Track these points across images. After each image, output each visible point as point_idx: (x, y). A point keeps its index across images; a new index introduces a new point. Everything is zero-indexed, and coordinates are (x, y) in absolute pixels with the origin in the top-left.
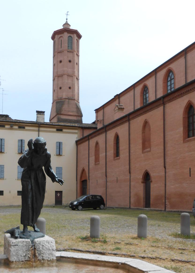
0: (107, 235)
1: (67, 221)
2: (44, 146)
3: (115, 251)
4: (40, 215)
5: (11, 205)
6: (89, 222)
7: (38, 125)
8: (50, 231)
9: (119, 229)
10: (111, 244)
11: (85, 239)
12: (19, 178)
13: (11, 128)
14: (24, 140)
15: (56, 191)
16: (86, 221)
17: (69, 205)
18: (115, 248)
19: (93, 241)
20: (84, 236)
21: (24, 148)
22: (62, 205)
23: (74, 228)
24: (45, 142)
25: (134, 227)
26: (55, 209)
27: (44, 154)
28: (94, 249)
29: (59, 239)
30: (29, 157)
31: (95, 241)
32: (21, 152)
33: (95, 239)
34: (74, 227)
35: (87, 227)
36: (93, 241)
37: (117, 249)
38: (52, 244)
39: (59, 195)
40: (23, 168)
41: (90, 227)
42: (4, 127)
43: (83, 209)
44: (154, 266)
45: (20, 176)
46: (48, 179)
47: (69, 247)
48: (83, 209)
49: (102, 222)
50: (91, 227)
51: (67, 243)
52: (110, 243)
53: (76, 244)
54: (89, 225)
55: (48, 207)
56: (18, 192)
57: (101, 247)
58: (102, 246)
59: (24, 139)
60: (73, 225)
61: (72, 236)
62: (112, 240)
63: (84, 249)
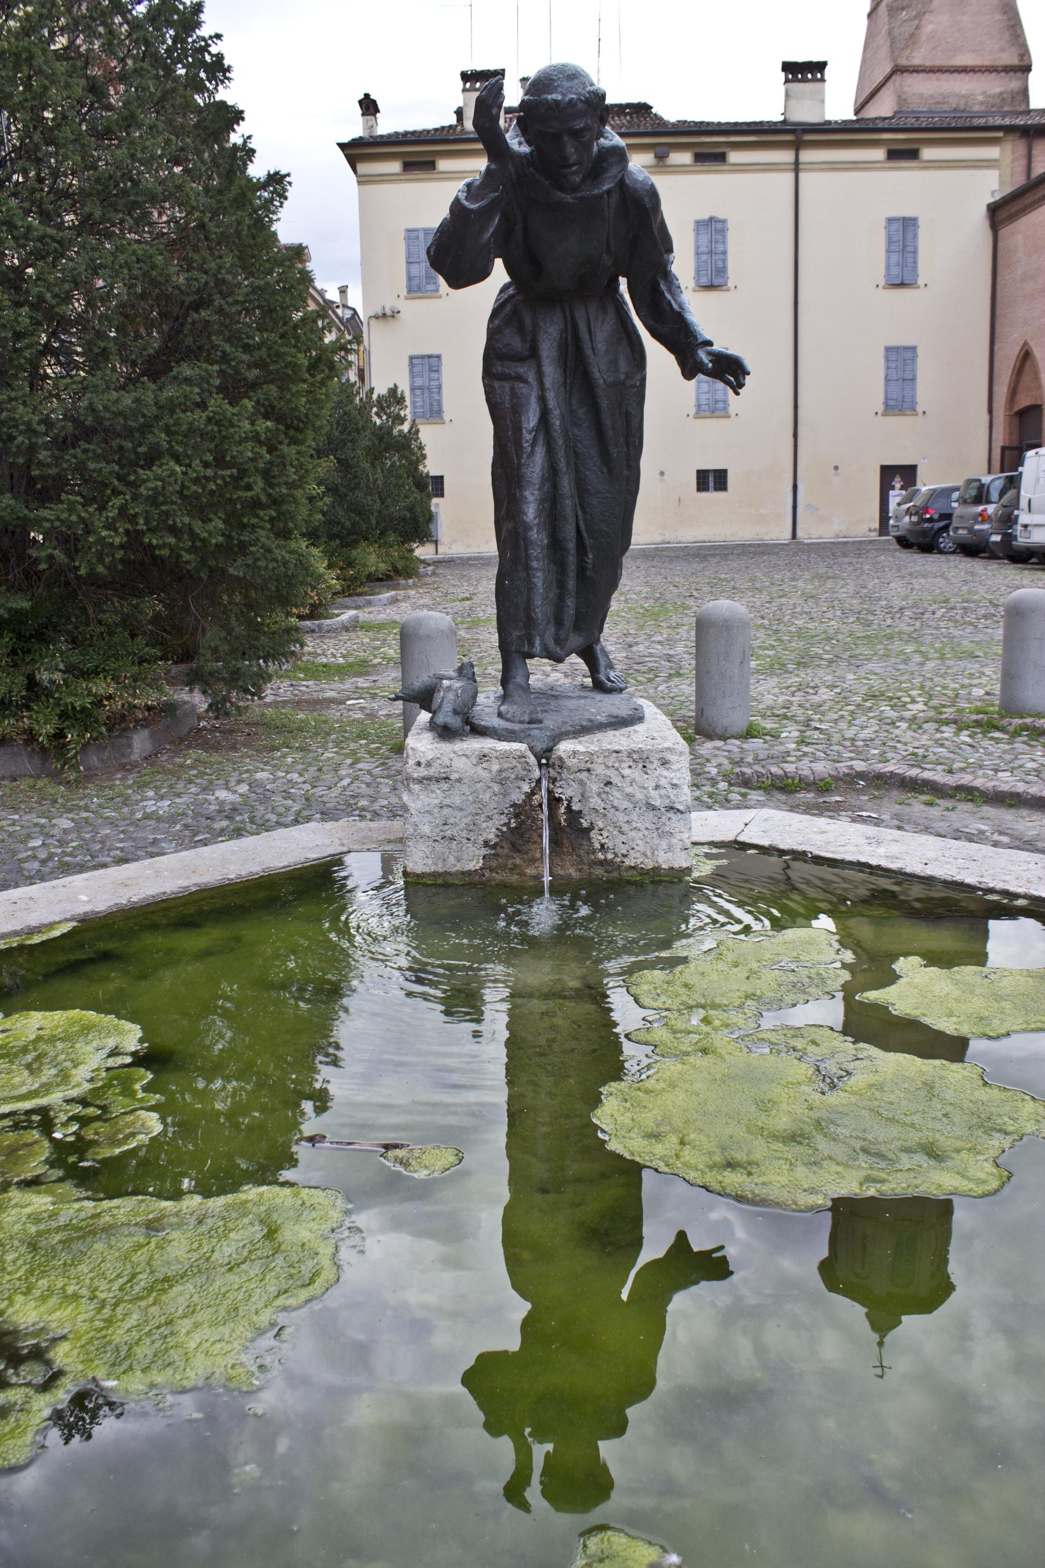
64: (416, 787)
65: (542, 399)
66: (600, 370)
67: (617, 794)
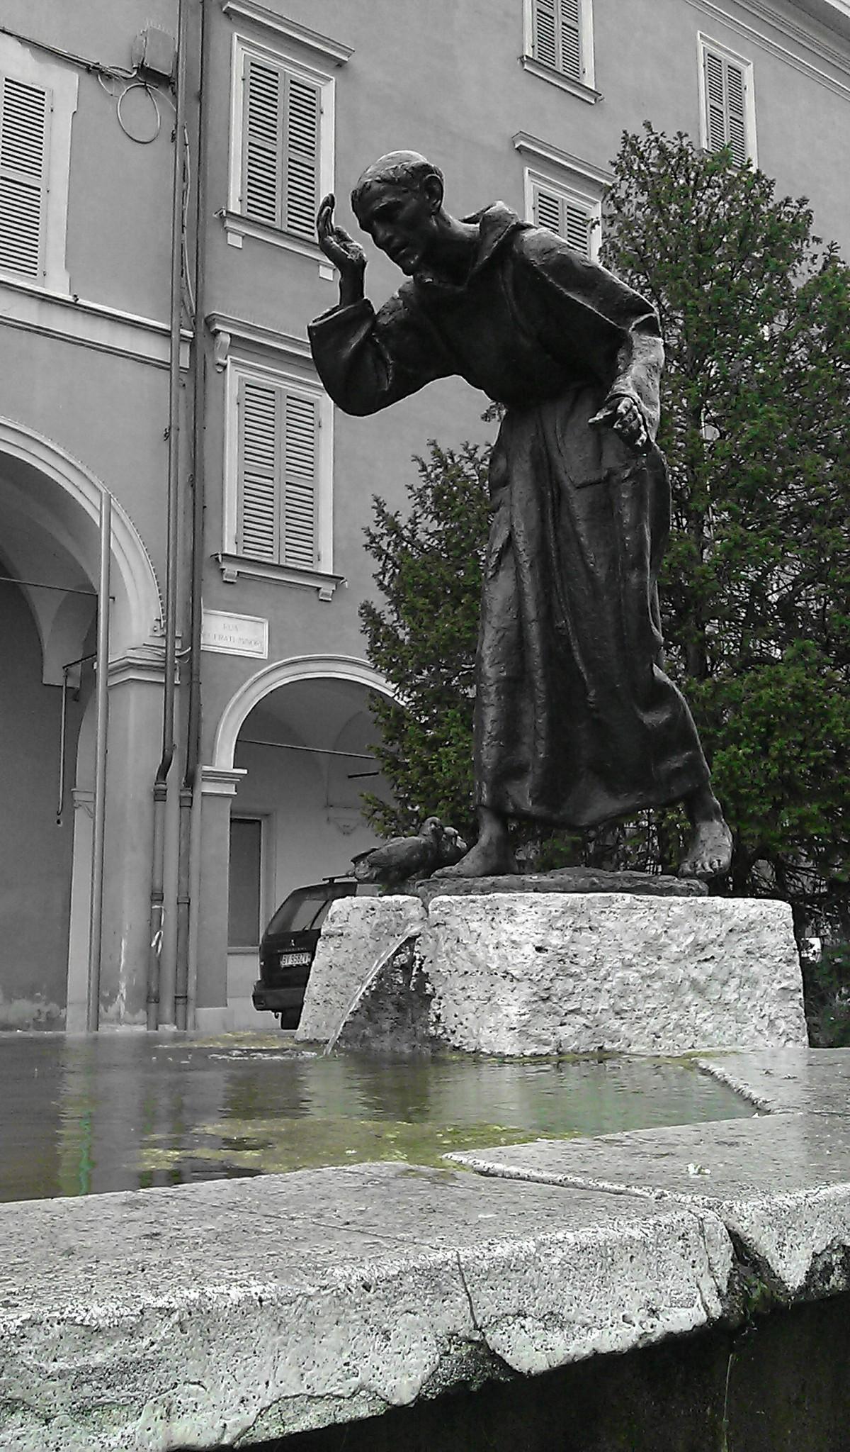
67: (462, 953)
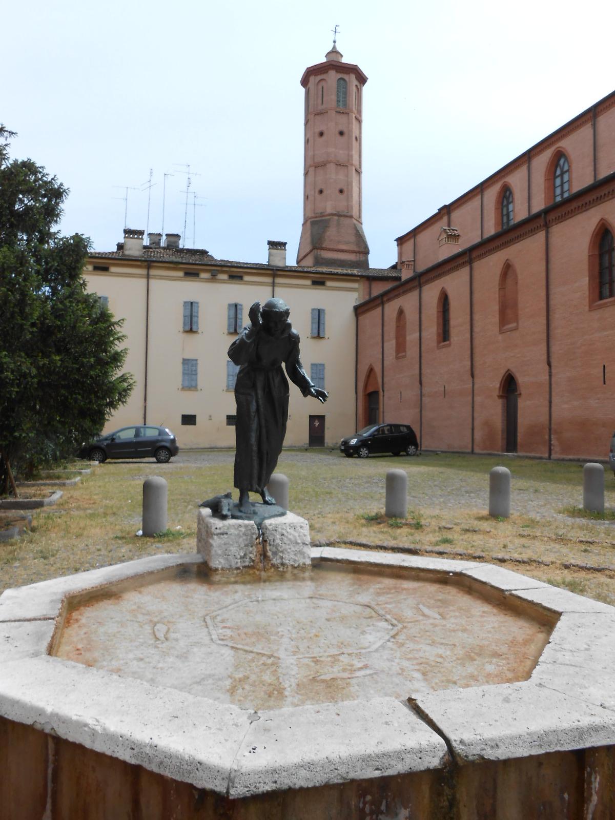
0: (422, 512)
1: (334, 481)
2: (286, 318)
3: (439, 545)
4: (276, 468)
5: (213, 445)
6: (383, 484)
7: (272, 272)
8: (299, 502)
9: (449, 499)
10: (431, 532)
11: (375, 520)
12: (231, 387)
13: (212, 279)
14: (241, 305)
15: (311, 417)
16: (377, 481)
17: (340, 447)
18: (440, 539)
19: (392, 525)
20: (373, 514)
21: (241, 322)
22: (324, 446)
23: (349, 497)
24: (288, 310)
25: (482, 493)
26: (308, 454)
27: (286, 335)
28: (394, 542)
29: (318, 519)
30: (251, 343)
31: (397, 524)
32: (236, 330)
33: (396, 520)
34: (351, 494)
35: (380, 493)
36: (392, 525)
37: (445, 543)
38: (302, 531)
39: (317, 424)
40: (239, 366)
41: (385, 494)
42: (198, 277)
43: (370, 455)
44: (525, 578)
45: (231, 382)
46: (294, 390)
47: (339, 537)
48: (370, 455)
49: (412, 482)
50: (387, 494)
51: (334, 528)
52: (429, 530)
53: (355, 531)
54: (384, 491)
55: (293, 450)
56: (229, 417)
57: (410, 537)
58: (412, 535)
59: (240, 303)
60: (348, 489)
61: (346, 514)
62: (434, 523)
63: (373, 542)
64: (215, 537)
65: (257, 402)
66: (276, 393)
